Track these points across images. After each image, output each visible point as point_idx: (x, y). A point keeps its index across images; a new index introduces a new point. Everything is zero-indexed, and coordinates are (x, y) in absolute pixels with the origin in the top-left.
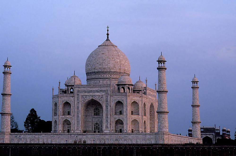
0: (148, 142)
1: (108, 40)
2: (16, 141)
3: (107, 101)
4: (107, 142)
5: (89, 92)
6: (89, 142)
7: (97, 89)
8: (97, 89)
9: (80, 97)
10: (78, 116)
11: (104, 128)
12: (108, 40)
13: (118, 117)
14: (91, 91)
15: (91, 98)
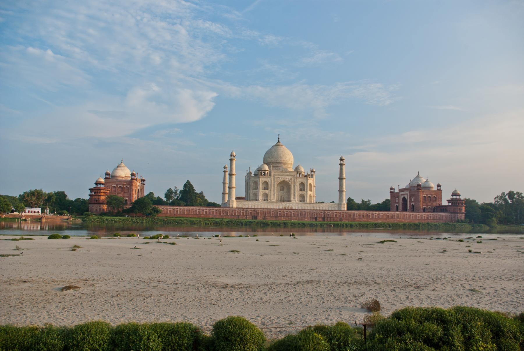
0: (333, 209)
1: (279, 142)
2: (240, 206)
3: (294, 182)
4: (306, 208)
5: (282, 175)
6: (294, 208)
7: (287, 174)
8: (287, 174)
9: (276, 178)
10: (274, 191)
11: (292, 199)
12: (279, 142)
13: (301, 192)
14: (283, 175)
15: (283, 180)
